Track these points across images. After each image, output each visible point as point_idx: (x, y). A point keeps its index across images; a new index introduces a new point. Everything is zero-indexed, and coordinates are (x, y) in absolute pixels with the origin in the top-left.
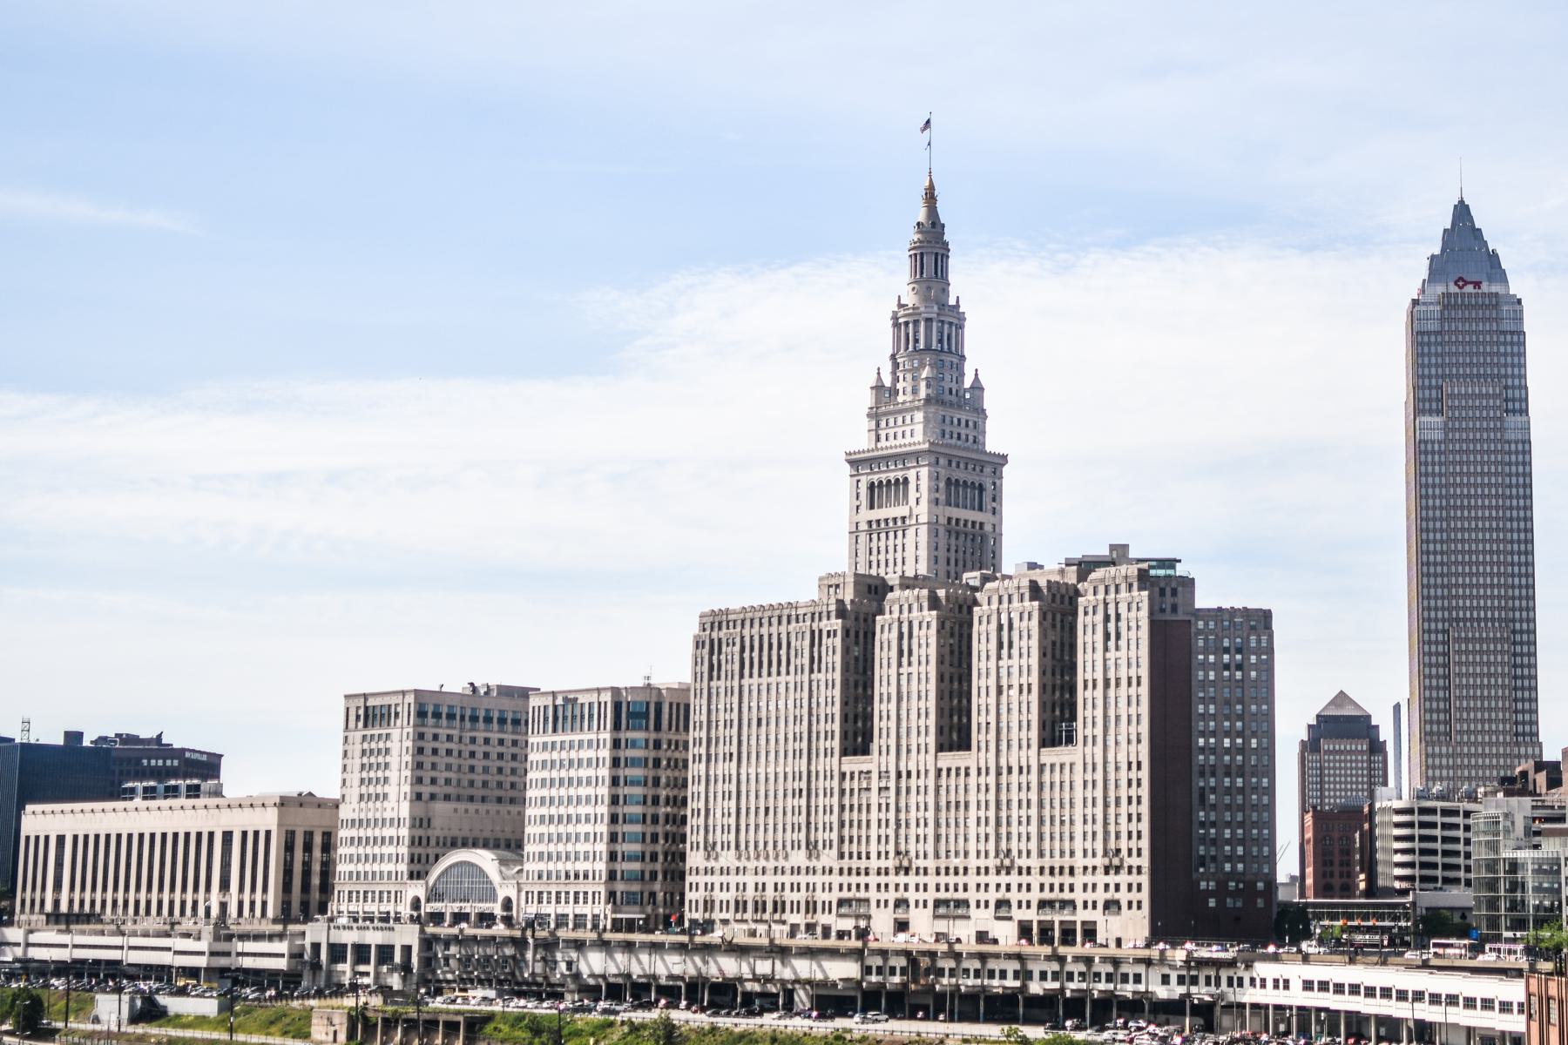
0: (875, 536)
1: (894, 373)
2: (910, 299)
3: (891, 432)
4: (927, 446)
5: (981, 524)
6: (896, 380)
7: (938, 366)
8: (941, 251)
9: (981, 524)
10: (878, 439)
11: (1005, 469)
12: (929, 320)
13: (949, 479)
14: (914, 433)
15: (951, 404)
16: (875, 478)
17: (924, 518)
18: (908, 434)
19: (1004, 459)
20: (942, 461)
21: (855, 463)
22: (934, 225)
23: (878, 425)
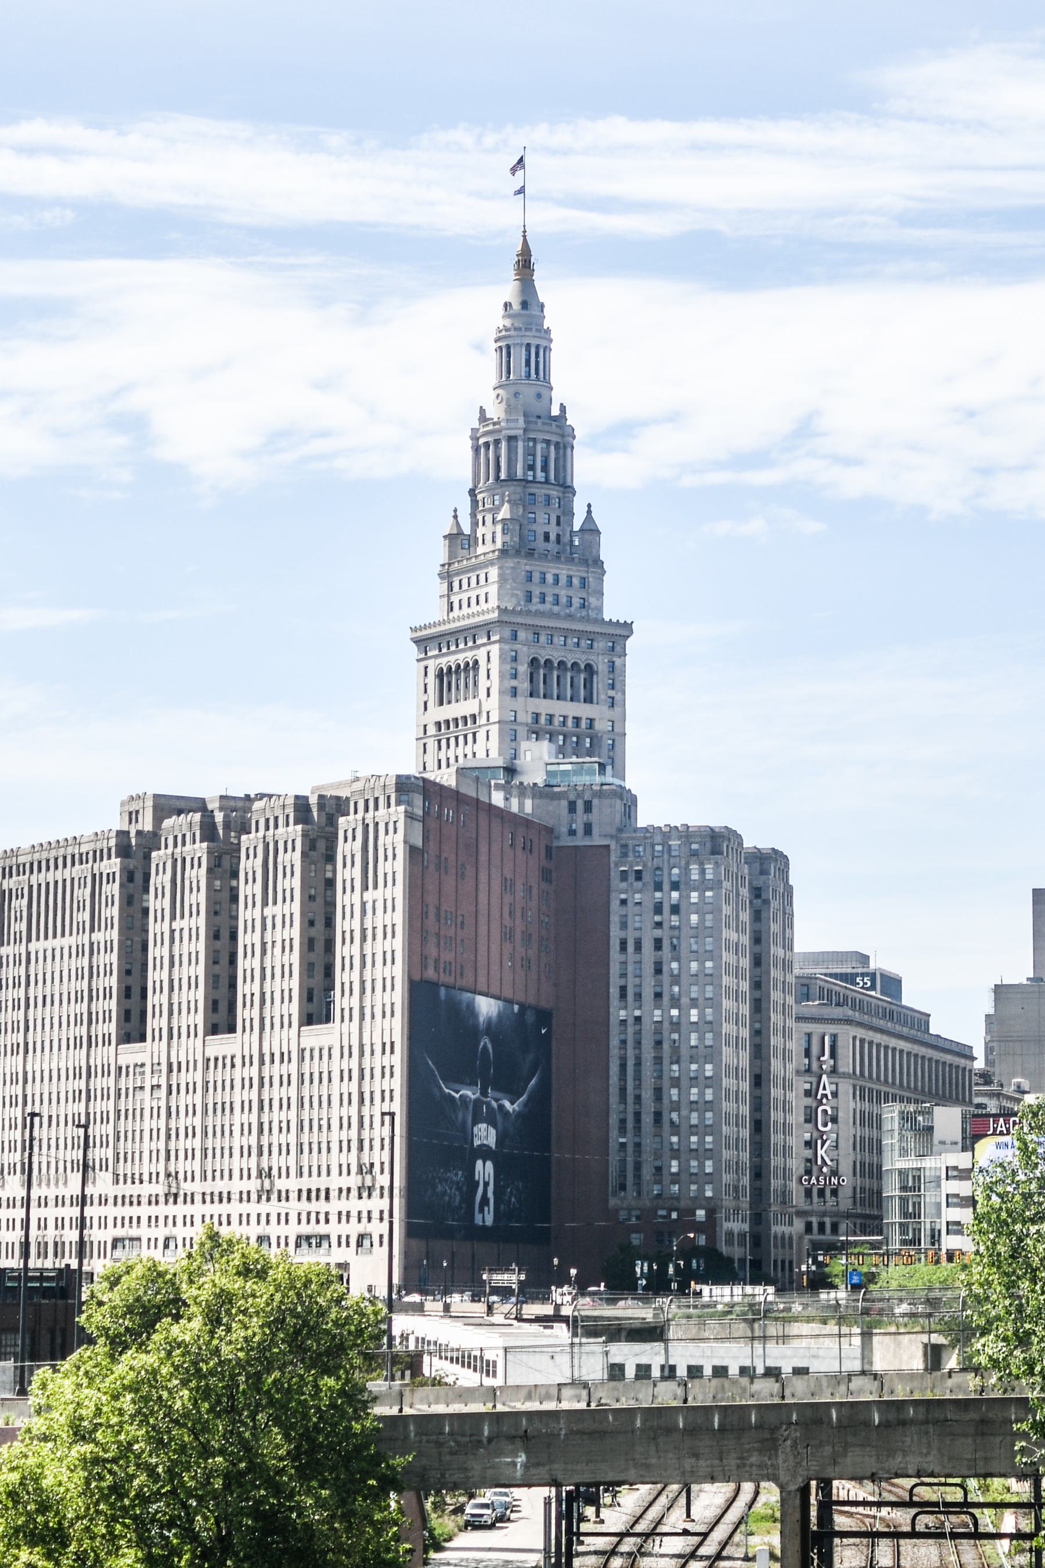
0: (444, 743)
1: (473, 515)
2: (495, 412)
3: (464, 597)
4: (495, 615)
5: (592, 720)
6: (475, 524)
7: (526, 502)
8: (534, 342)
9: (592, 720)
10: (451, 609)
11: (629, 642)
12: (511, 439)
13: (534, 662)
14: (487, 596)
15: (544, 556)
16: (443, 662)
17: (495, 717)
18: (482, 599)
19: (627, 628)
20: (522, 635)
21: (422, 643)
22: (524, 305)
23: (451, 588)
